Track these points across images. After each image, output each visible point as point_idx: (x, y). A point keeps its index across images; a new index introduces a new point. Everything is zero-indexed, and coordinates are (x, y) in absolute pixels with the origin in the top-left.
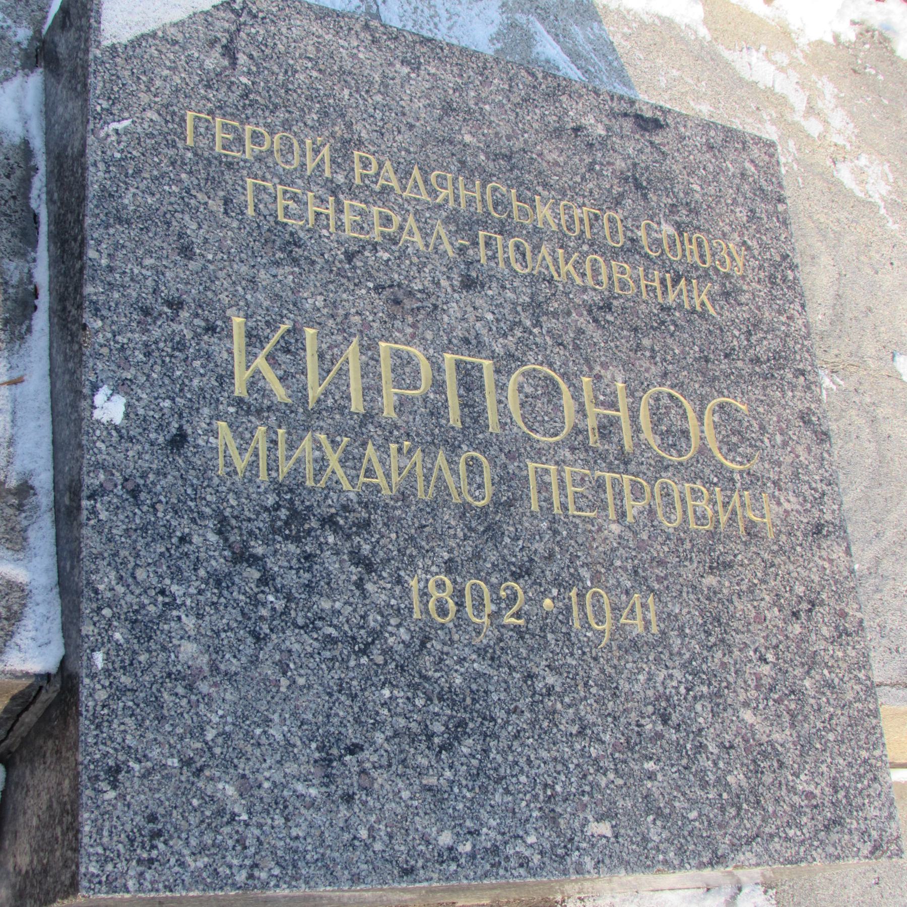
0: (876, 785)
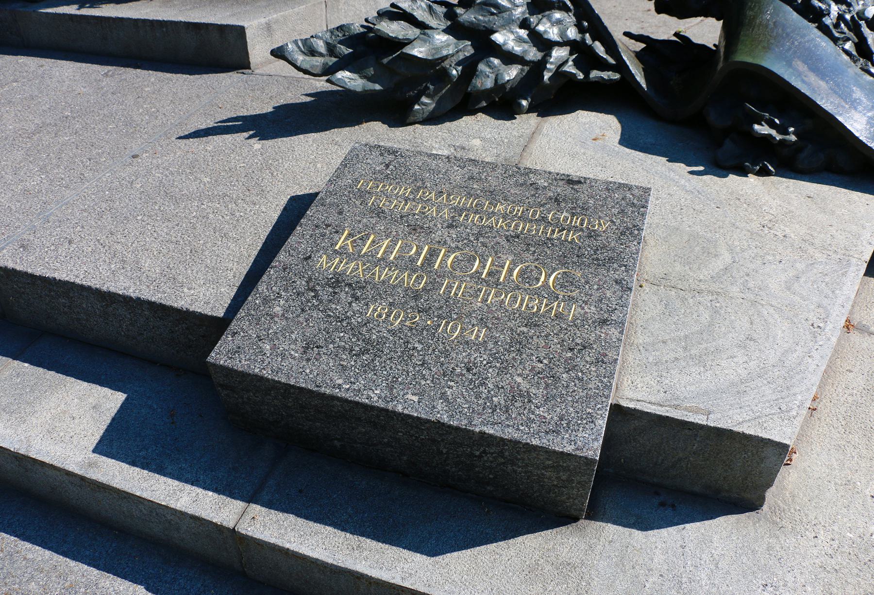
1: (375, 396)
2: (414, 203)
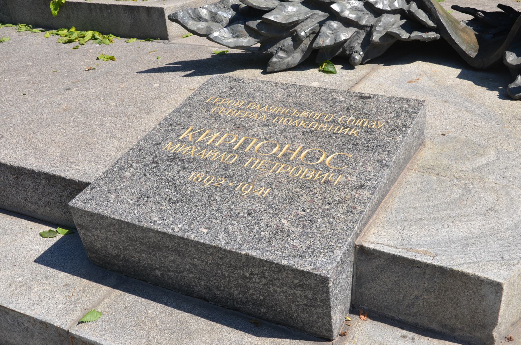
0: (331, 254)
1: (177, 229)
2: (243, 111)
